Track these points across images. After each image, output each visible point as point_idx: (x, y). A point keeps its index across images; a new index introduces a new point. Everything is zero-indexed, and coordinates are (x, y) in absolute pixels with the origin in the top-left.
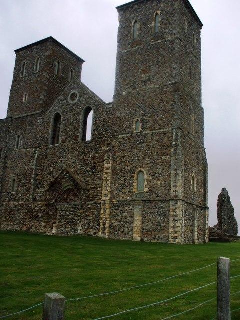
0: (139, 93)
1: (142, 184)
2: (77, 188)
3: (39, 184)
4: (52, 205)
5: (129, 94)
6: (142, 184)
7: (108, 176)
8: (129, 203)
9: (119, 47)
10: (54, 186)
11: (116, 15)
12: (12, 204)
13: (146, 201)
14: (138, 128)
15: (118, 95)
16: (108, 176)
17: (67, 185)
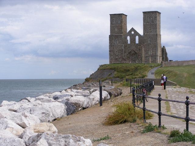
0: (149, 34)
1: (150, 53)
2: (136, 53)
3: (125, 52)
4: (128, 57)
5: (147, 34)
6: (150, 53)
7: (143, 51)
8: (148, 56)
9: (144, 22)
10: (130, 53)
11: (142, 14)
12: (117, 57)
13: (151, 56)
14: (149, 42)
15: (144, 34)
16: (143, 51)
17: (133, 52)
